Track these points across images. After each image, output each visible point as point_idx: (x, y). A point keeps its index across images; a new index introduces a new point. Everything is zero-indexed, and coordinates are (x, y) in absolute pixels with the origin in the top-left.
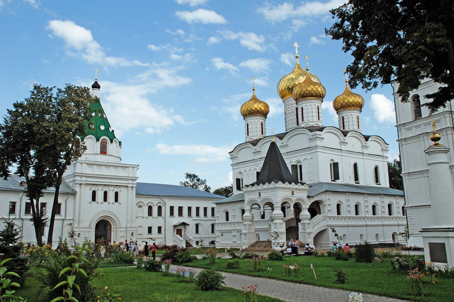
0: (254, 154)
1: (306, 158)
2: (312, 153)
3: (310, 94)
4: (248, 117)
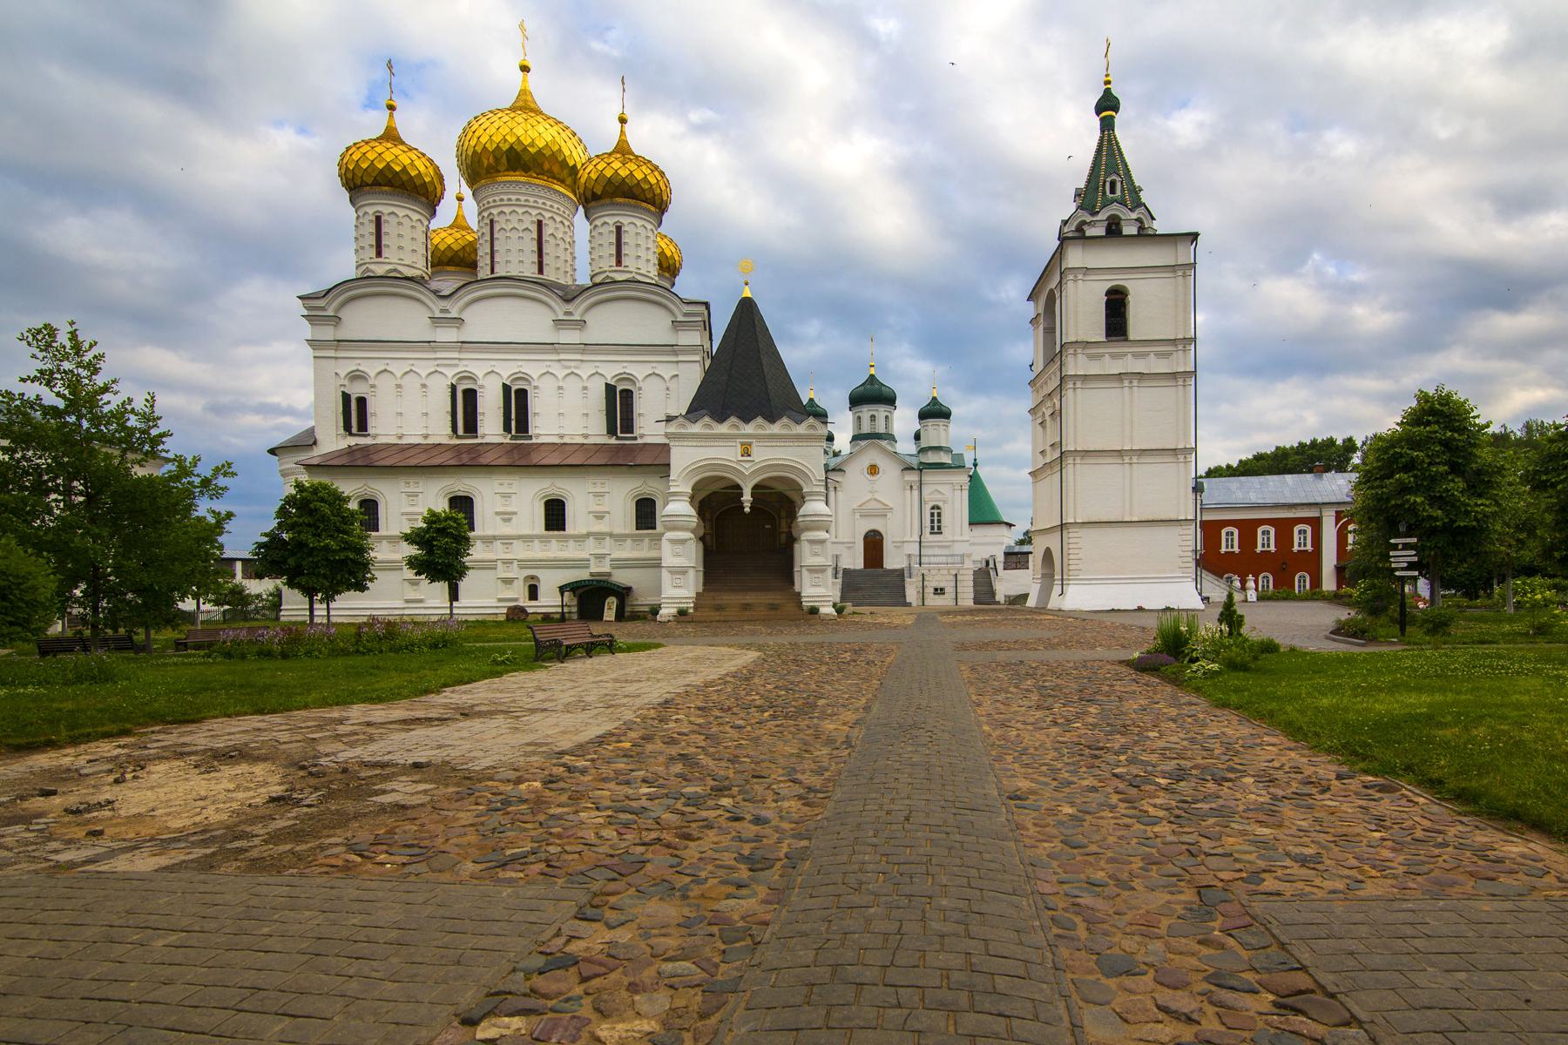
0: (434, 322)
1: (597, 373)
2: (677, 362)
3: (649, 196)
4: (386, 193)
